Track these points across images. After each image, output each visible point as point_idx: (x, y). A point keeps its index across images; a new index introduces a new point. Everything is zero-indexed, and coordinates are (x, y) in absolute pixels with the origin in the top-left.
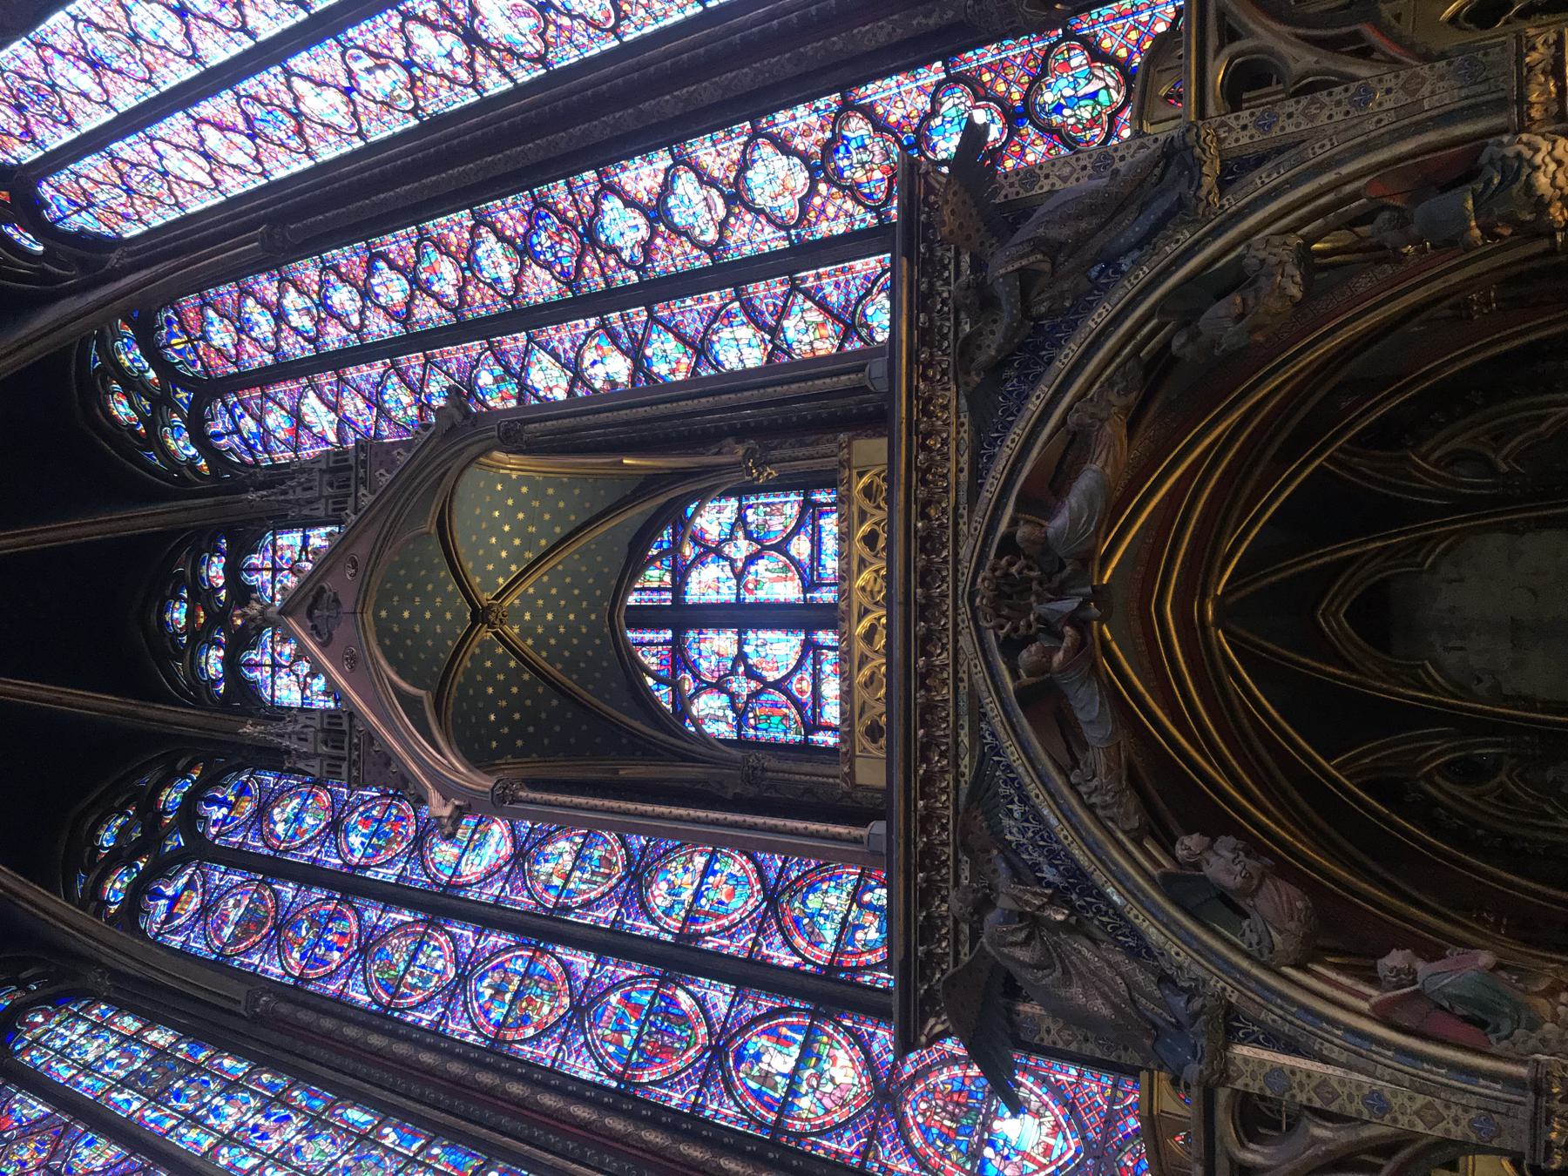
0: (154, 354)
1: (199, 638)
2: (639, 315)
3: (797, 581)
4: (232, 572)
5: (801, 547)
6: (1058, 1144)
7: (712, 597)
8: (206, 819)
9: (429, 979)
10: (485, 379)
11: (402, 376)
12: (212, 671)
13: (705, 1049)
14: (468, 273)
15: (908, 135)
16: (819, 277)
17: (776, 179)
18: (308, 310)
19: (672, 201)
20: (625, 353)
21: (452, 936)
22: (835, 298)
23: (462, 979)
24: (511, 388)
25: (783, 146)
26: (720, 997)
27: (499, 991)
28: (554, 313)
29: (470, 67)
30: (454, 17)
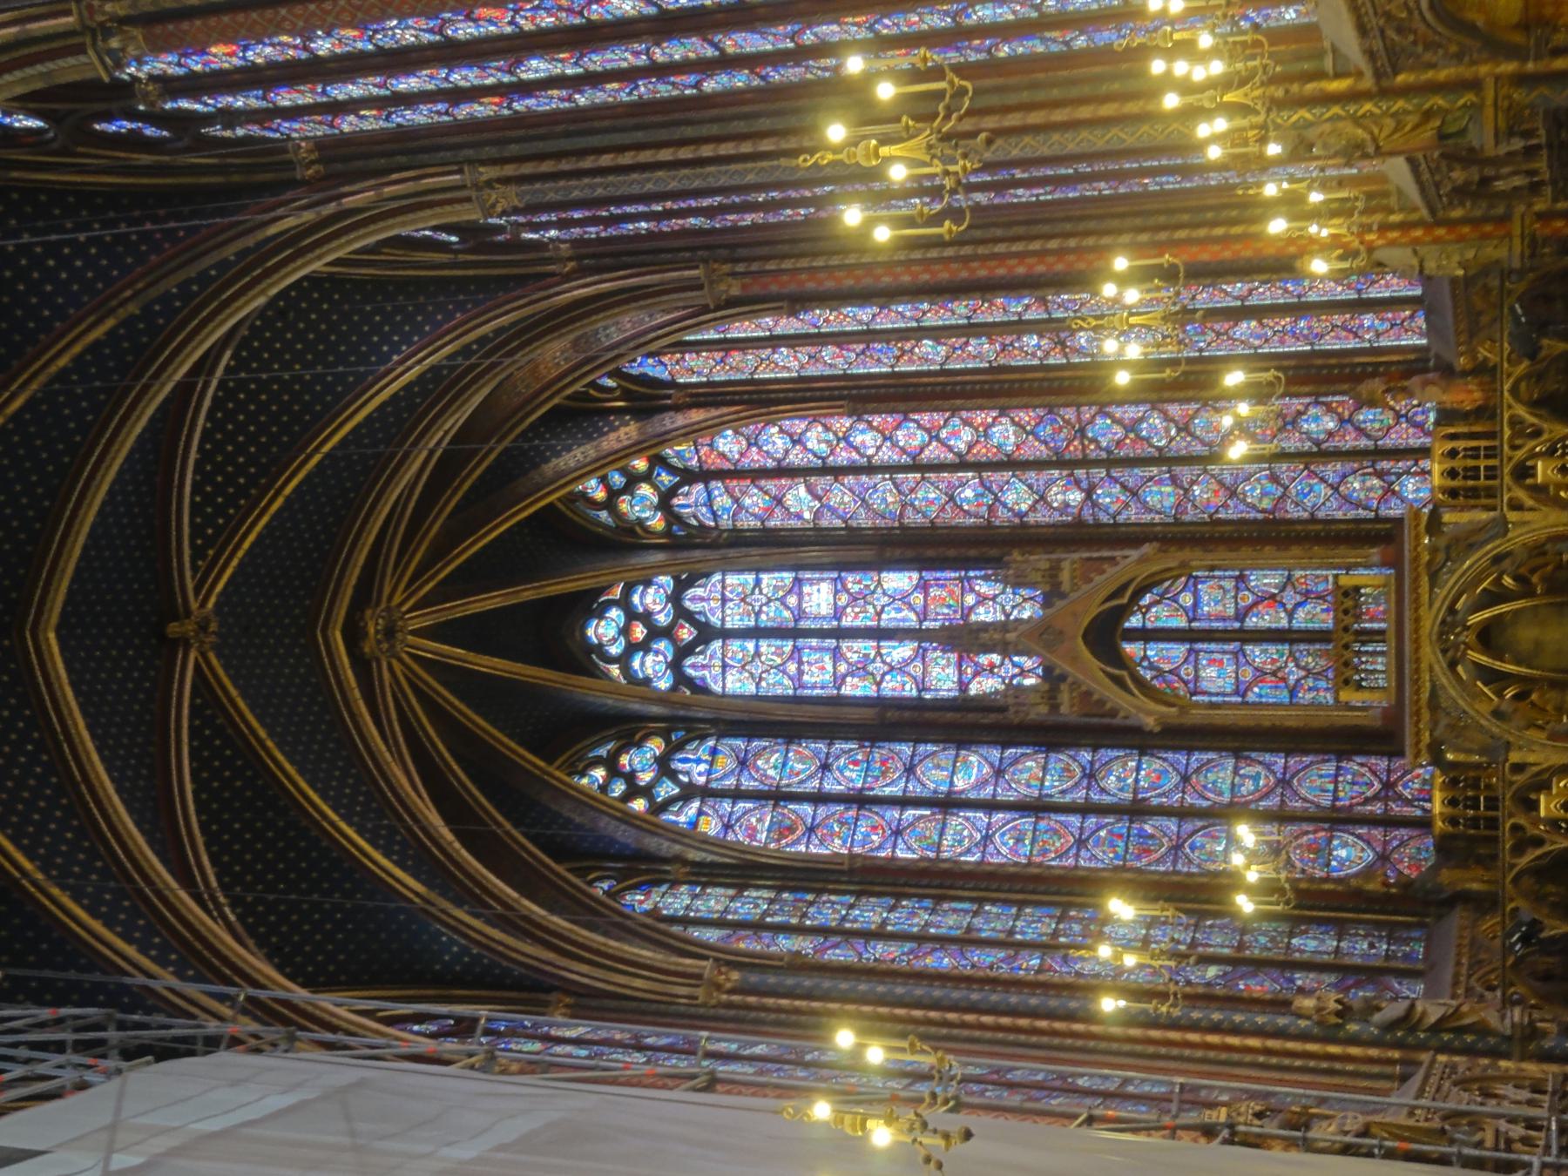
3: (1184, 618)
4: (675, 598)
5: (1187, 599)
6: (1364, 855)
8: (687, 773)
9: (960, 842)
10: (969, 493)
11: (896, 486)
12: (650, 672)
13: (1170, 849)
15: (1289, 419)
18: (828, 442)
21: (967, 819)
23: (987, 838)
24: (989, 499)
26: (1171, 825)
27: (1019, 840)
28: (1039, 465)
29: (1047, 354)
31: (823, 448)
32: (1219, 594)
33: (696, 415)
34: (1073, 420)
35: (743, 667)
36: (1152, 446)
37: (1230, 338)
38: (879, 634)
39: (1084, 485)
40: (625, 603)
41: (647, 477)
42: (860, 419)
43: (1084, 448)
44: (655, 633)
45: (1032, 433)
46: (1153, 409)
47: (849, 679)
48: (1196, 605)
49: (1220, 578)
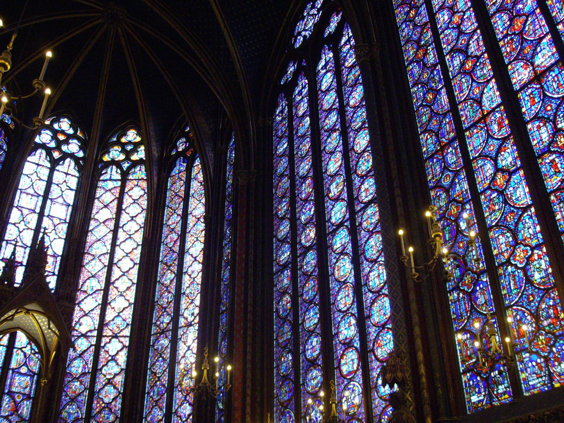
0: (140, 162)
1: (55, 133)
2: (94, 341)
3: (15, 367)
4: (72, 156)
7: (17, 340)
14: (120, 293)
16: (86, 396)
17: (109, 394)
19: (114, 364)
20: (87, 333)
22: (80, 399)
24: (90, 292)
25: (115, 399)
30: (167, 331)
31: (126, 228)
32: (23, 385)
33: (155, 179)
34: (121, 334)
35: (36, 172)
36: (103, 366)
37: (153, 407)
38: (37, 231)
39: (89, 334)
40: (74, 136)
41: (128, 159)
42: (138, 245)
43: (108, 337)
44: (59, 144)
45: (118, 316)
46: (122, 370)
47: (20, 212)
48: (21, 374)
49: (31, 387)
